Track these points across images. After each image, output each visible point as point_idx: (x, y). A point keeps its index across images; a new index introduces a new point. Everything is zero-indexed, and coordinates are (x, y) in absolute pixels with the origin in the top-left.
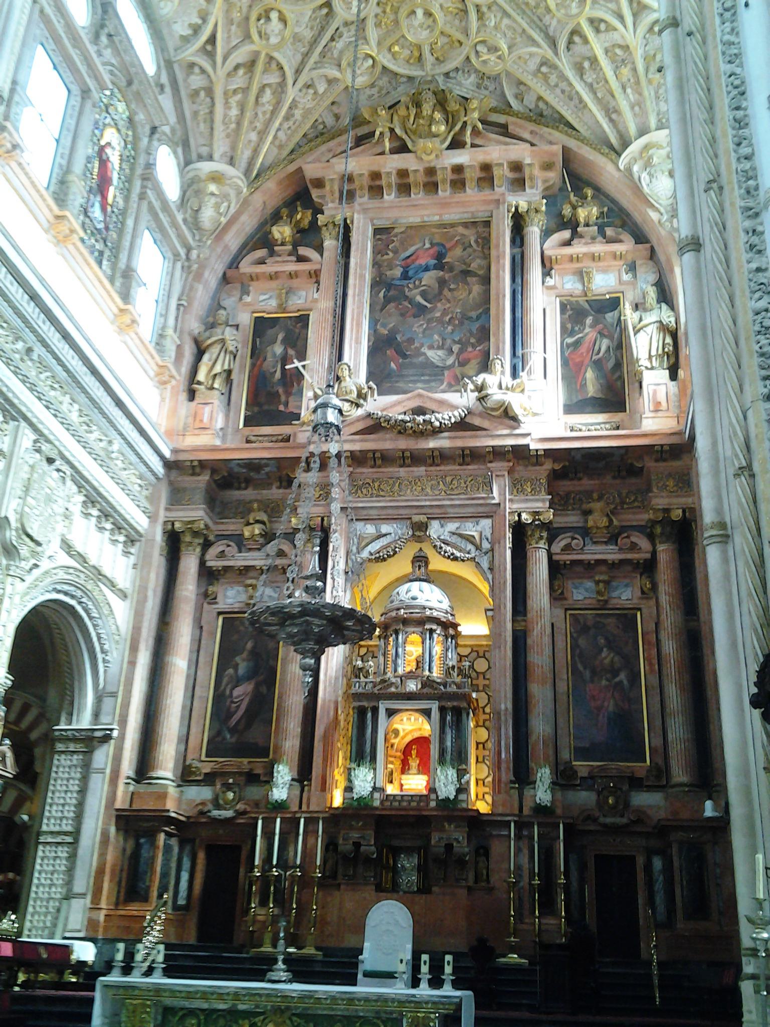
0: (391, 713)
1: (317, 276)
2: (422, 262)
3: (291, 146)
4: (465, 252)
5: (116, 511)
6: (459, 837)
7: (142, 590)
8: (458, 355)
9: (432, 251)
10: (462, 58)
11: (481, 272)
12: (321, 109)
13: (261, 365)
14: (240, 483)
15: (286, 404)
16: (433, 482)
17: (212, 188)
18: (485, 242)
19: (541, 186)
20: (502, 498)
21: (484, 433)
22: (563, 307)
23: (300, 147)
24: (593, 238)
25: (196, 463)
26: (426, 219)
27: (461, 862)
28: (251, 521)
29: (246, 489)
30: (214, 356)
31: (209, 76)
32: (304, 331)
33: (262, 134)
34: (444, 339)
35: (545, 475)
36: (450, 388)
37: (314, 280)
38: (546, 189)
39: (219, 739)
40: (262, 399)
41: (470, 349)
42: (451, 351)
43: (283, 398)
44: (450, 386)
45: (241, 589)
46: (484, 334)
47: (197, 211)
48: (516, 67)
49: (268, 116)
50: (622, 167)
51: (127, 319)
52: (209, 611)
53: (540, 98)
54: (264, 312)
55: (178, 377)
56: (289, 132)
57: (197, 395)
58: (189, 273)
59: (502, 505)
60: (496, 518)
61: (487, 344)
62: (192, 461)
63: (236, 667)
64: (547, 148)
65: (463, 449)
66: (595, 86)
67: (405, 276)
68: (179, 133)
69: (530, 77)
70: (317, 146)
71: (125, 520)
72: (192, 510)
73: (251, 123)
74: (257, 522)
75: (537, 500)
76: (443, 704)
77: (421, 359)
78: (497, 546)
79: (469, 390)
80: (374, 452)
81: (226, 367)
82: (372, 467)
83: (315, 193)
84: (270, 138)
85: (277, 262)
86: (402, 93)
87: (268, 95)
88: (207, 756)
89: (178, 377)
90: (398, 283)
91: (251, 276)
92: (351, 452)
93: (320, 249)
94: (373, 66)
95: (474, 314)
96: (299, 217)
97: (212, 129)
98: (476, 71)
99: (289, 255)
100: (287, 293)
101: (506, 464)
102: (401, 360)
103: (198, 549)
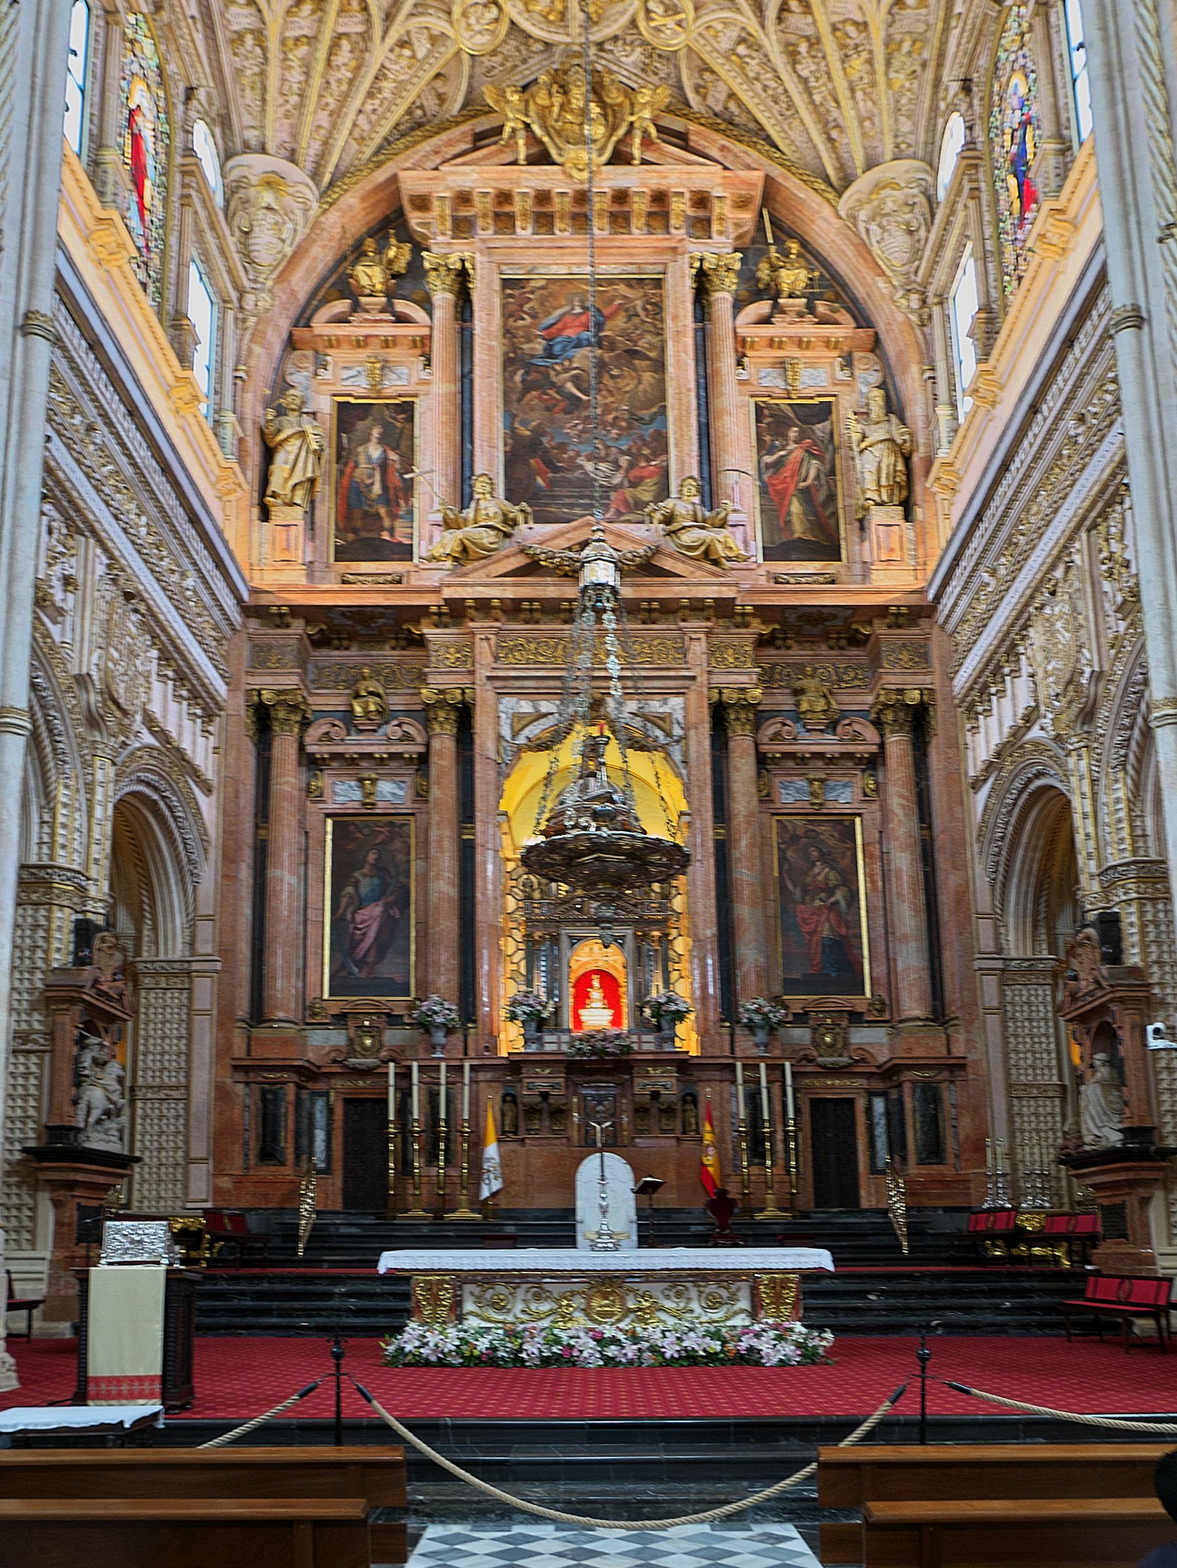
1: (423, 345)
2: (571, 333)
3: (378, 140)
4: (629, 325)
5: (194, 673)
6: (667, 1082)
8: (628, 471)
9: (583, 318)
10: (624, 20)
11: (652, 355)
12: (423, 82)
17: (268, 198)
18: (657, 309)
19: (733, 233)
22: (759, 409)
23: (389, 143)
24: (800, 315)
25: (285, 610)
26: (575, 270)
30: (292, 457)
31: (259, 11)
32: (408, 426)
33: (336, 115)
34: (607, 447)
36: (618, 517)
37: (419, 351)
38: (738, 238)
41: (643, 464)
42: (618, 467)
44: (619, 513)
46: (660, 444)
47: (247, 233)
48: (702, 42)
49: (344, 87)
50: (843, 214)
53: (732, 95)
56: (374, 117)
57: (274, 511)
58: (245, 329)
61: (663, 458)
64: (744, 174)
65: (650, 601)
66: (812, 84)
67: (549, 353)
68: (216, 101)
69: (721, 61)
70: (416, 143)
71: (203, 685)
73: (321, 96)
77: (577, 474)
80: (531, 600)
81: (309, 475)
82: (527, 622)
83: (414, 219)
84: (348, 124)
85: (367, 321)
86: (538, 69)
87: (344, 55)
89: (245, 486)
90: (540, 362)
91: (330, 341)
93: (426, 304)
94: (497, 20)
95: (645, 414)
96: (392, 253)
97: (264, 101)
98: (644, 43)
99: (382, 311)
100: (383, 368)
102: (550, 475)
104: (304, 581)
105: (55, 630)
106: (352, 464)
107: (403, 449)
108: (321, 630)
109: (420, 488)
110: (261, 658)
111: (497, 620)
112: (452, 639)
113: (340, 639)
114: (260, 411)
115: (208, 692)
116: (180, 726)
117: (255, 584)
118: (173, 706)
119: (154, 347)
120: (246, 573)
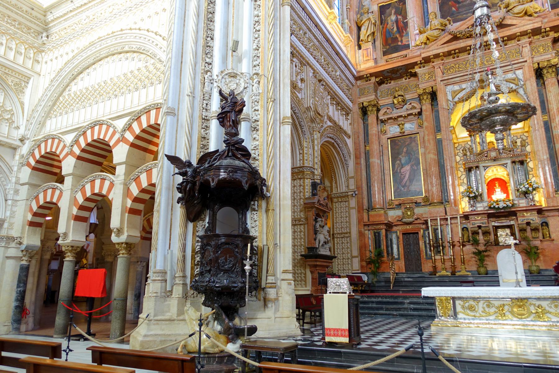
0: (486, 168)
5: (342, 101)
7: (356, 134)
13: (386, 27)
14: (387, 81)
15: (402, 41)
16: (487, 58)
20: (527, 58)
21: (514, 27)
25: (368, 75)
27: (535, 230)
28: (397, 96)
29: (390, 83)
32: (404, 6)
35: (551, 41)
39: (399, 190)
40: (390, 42)
43: (399, 39)
45: (397, 126)
51: (332, 17)
52: (384, 138)
54: (384, 2)
55: (353, 40)
59: (528, 61)
60: (526, 68)
62: (367, 75)
63: (400, 160)
71: (345, 104)
72: (370, 96)
74: (399, 96)
75: (547, 55)
76: (514, 159)
77: (468, 2)
78: (528, 83)
79: (502, 8)
80: (455, 50)
81: (372, 31)
82: (454, 58)
88: (394, 198)
89: (353, 40)
92: (443, 53)
101: (528, 40)
103: (375, 113)
104: (373, 65)
105: (299, 95)
106: (386, 24)
107: (403, 14)
108: (381, 79)
109: (411, 24)
110: (362, 93)
111: (442, 60)
112: (427, 71)
113: (387, 81)
114: (355, 16)
115: (347, 106)
116: (339, 118)
117: (359, 69)
118: (336, 113)
119: (321, 5)
120: (356, 67)
